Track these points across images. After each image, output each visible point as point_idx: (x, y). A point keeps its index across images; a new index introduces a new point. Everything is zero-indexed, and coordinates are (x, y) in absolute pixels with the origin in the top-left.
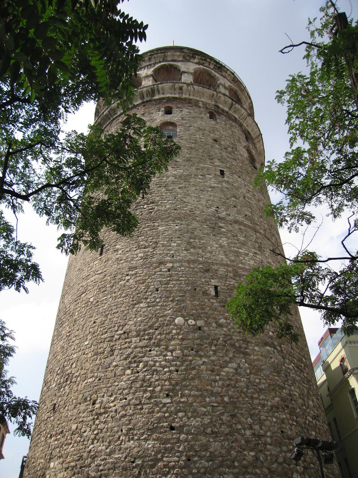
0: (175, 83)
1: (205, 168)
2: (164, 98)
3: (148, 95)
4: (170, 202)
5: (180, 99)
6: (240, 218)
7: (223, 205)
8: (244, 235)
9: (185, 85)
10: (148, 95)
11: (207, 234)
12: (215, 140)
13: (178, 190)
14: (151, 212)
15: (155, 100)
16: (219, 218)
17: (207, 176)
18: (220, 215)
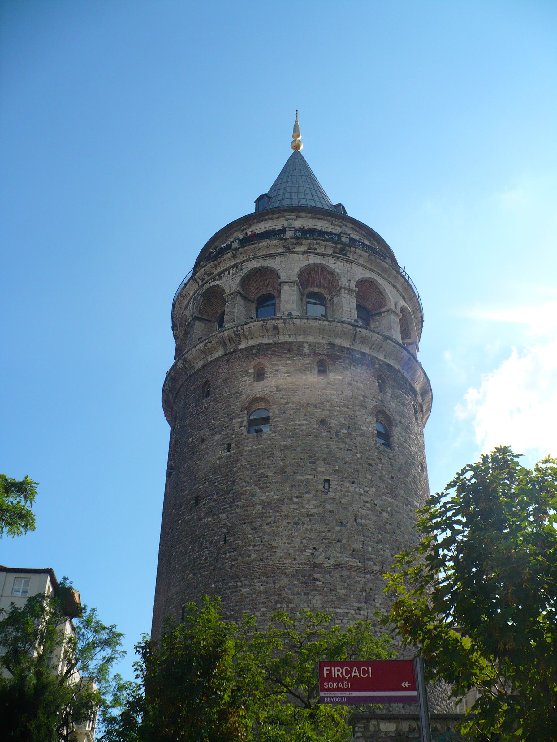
0: (266, 320)
1: (302, 482)
2: (252, 347)
3: (232, 342)
4: (256, 548)
5: (276, 344)
6: (345, 559)
7: (322, 543)
8: (346, 585)
9: (281, 321)
10: (232, 342)
11: (298, 594)
12: (322, 422)
13: (266, 528)
14: (233, 565)
15: (241, 349)
16: (316, 565)
17: (305, 495)
18: (317, 561)
